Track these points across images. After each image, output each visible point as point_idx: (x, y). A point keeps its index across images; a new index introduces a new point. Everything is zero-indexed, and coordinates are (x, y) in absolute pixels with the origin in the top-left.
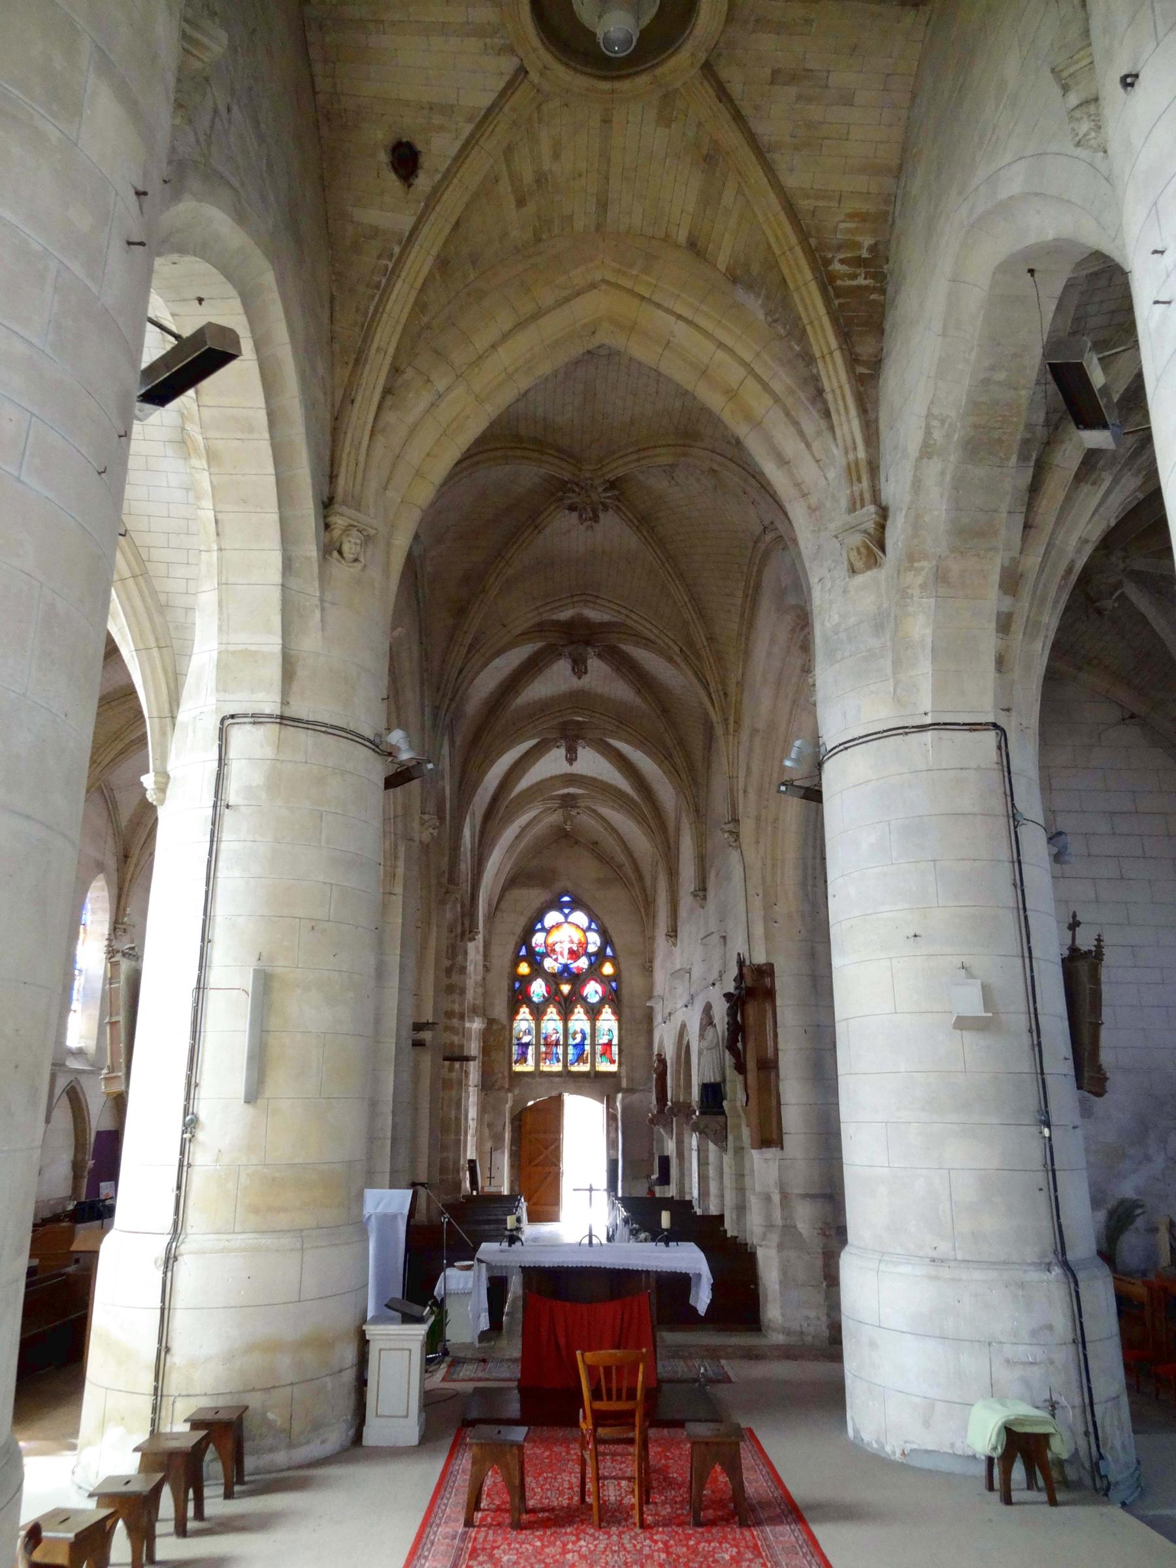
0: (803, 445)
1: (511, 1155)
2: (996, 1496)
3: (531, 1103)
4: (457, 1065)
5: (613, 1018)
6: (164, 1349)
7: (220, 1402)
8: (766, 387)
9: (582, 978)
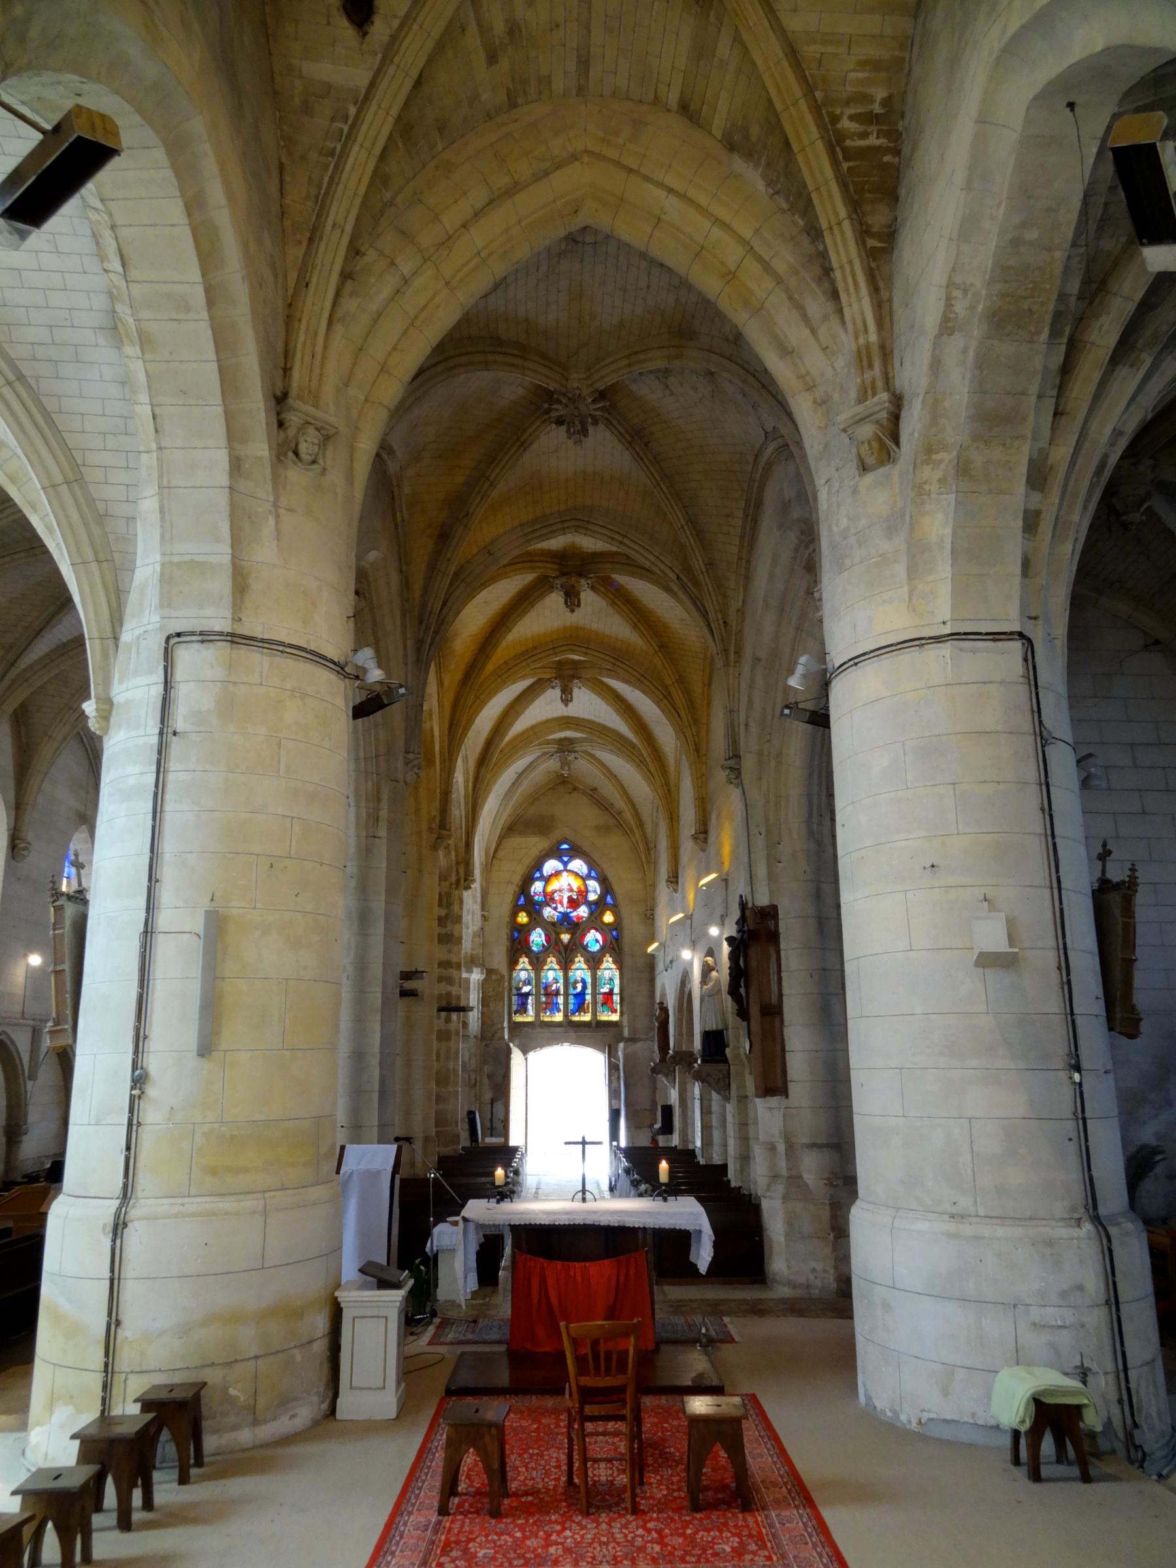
0: (808, 332)
2: (1021, 1473)
4: (454, 1016)
6: (114, 1322)
7: (177, 1379)
8: (767, 267)
9: (582, 927)
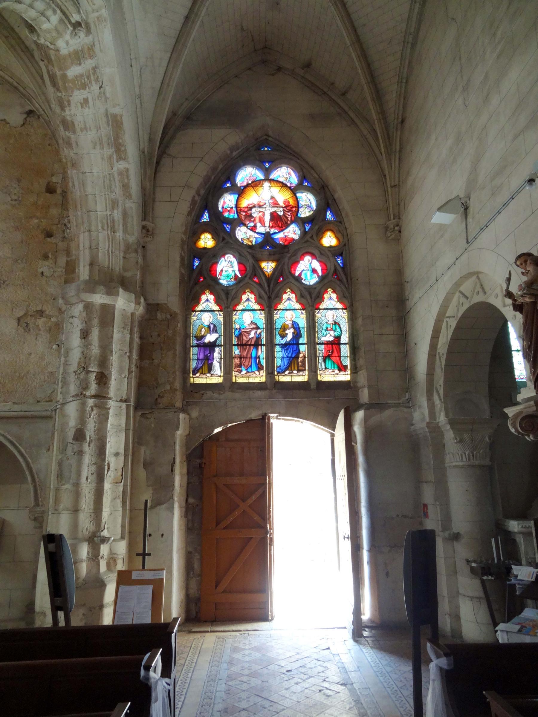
1: (189, 511)
3: (216, 431)
5: (339, 305)
9: (291, 251)
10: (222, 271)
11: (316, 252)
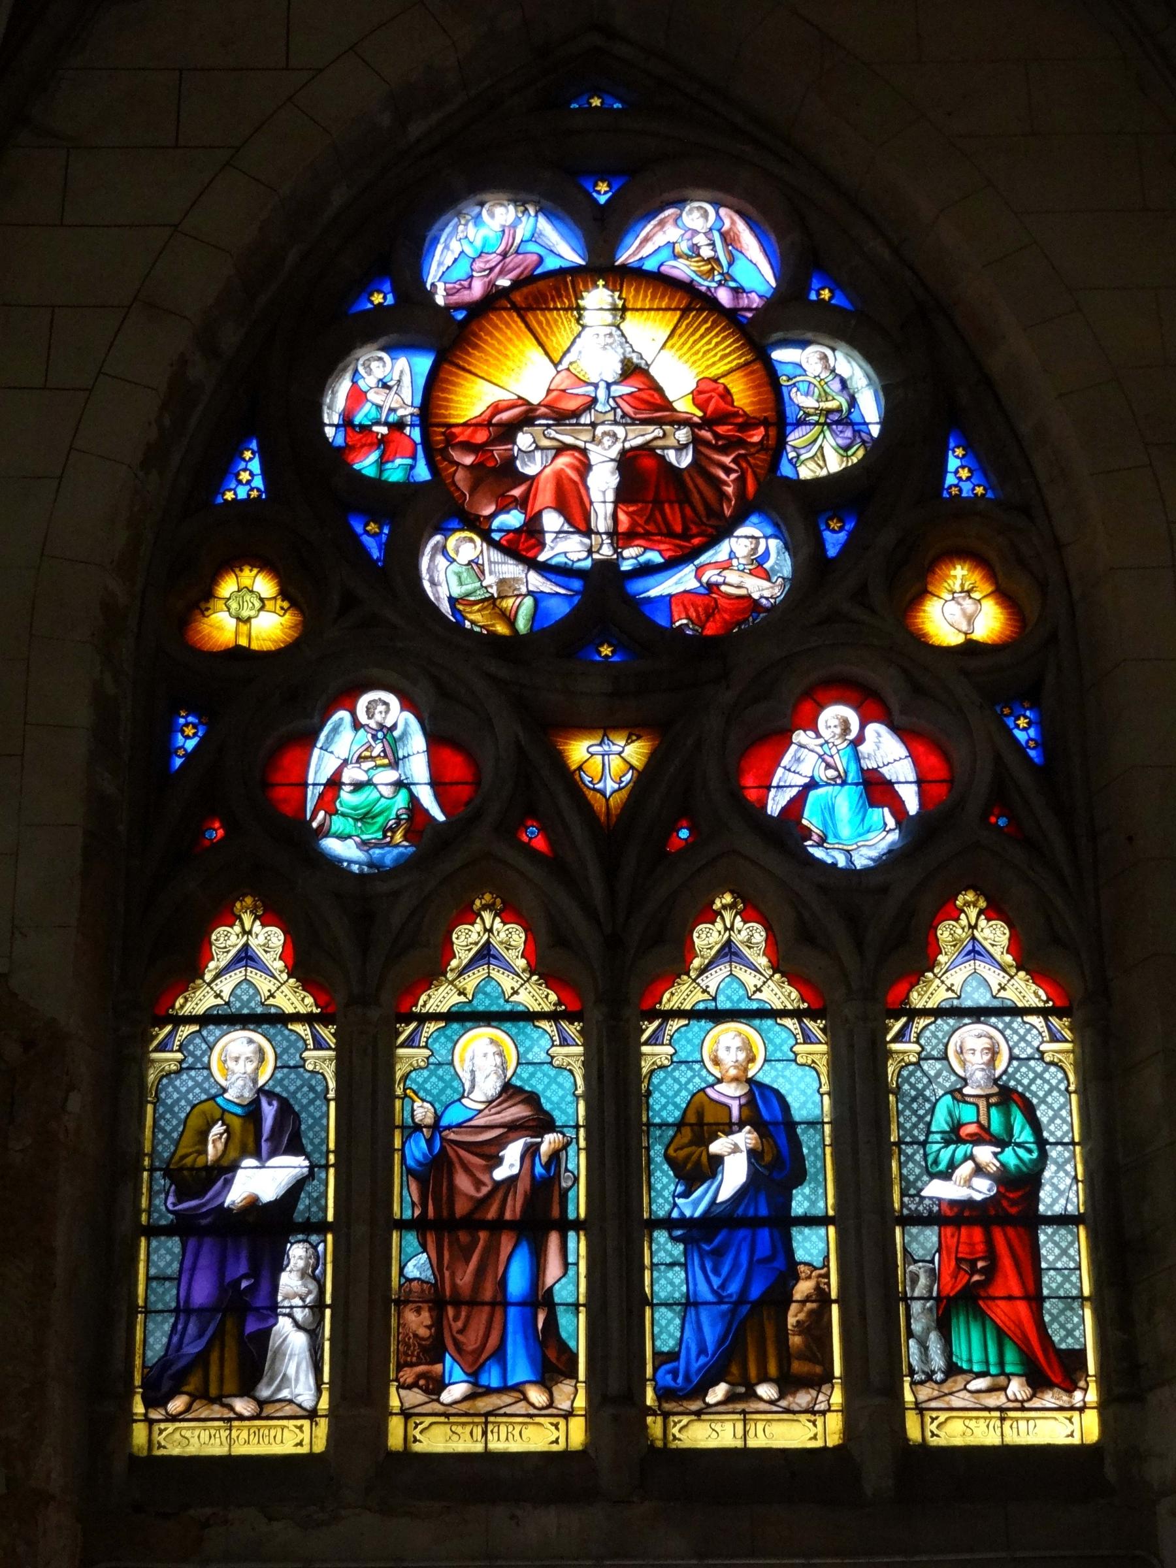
10: (334, 783)
11: (887, 680)
